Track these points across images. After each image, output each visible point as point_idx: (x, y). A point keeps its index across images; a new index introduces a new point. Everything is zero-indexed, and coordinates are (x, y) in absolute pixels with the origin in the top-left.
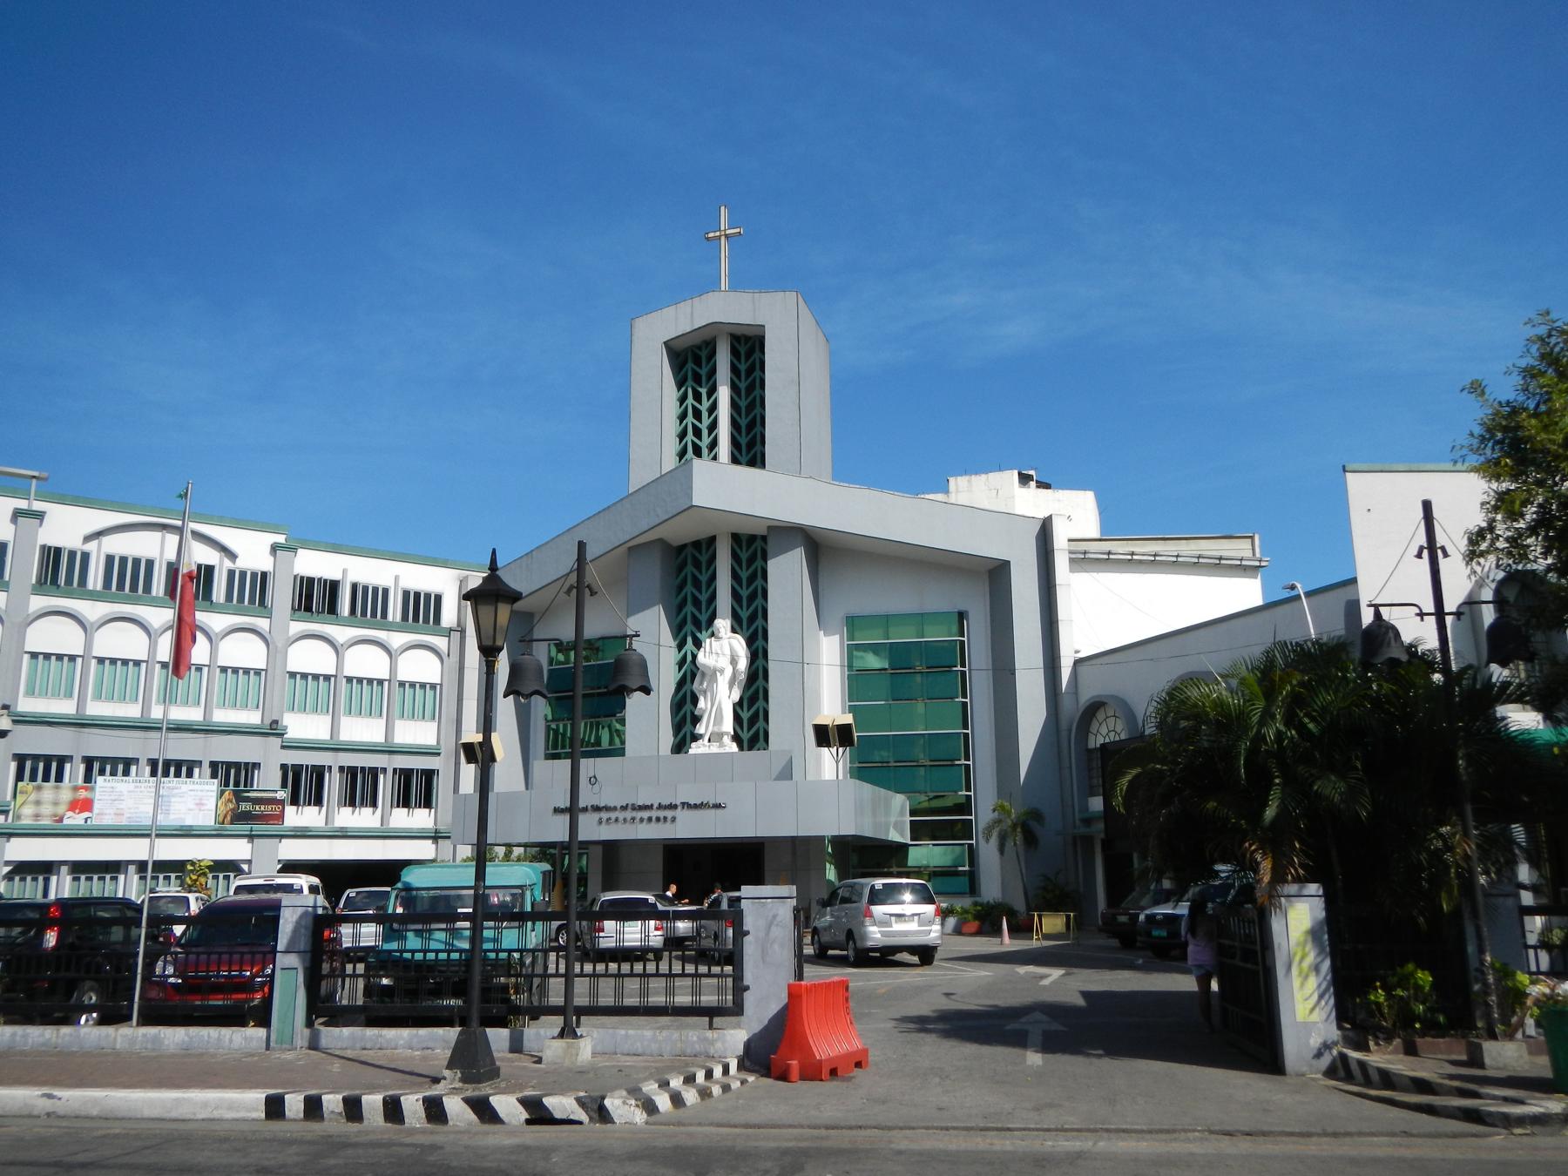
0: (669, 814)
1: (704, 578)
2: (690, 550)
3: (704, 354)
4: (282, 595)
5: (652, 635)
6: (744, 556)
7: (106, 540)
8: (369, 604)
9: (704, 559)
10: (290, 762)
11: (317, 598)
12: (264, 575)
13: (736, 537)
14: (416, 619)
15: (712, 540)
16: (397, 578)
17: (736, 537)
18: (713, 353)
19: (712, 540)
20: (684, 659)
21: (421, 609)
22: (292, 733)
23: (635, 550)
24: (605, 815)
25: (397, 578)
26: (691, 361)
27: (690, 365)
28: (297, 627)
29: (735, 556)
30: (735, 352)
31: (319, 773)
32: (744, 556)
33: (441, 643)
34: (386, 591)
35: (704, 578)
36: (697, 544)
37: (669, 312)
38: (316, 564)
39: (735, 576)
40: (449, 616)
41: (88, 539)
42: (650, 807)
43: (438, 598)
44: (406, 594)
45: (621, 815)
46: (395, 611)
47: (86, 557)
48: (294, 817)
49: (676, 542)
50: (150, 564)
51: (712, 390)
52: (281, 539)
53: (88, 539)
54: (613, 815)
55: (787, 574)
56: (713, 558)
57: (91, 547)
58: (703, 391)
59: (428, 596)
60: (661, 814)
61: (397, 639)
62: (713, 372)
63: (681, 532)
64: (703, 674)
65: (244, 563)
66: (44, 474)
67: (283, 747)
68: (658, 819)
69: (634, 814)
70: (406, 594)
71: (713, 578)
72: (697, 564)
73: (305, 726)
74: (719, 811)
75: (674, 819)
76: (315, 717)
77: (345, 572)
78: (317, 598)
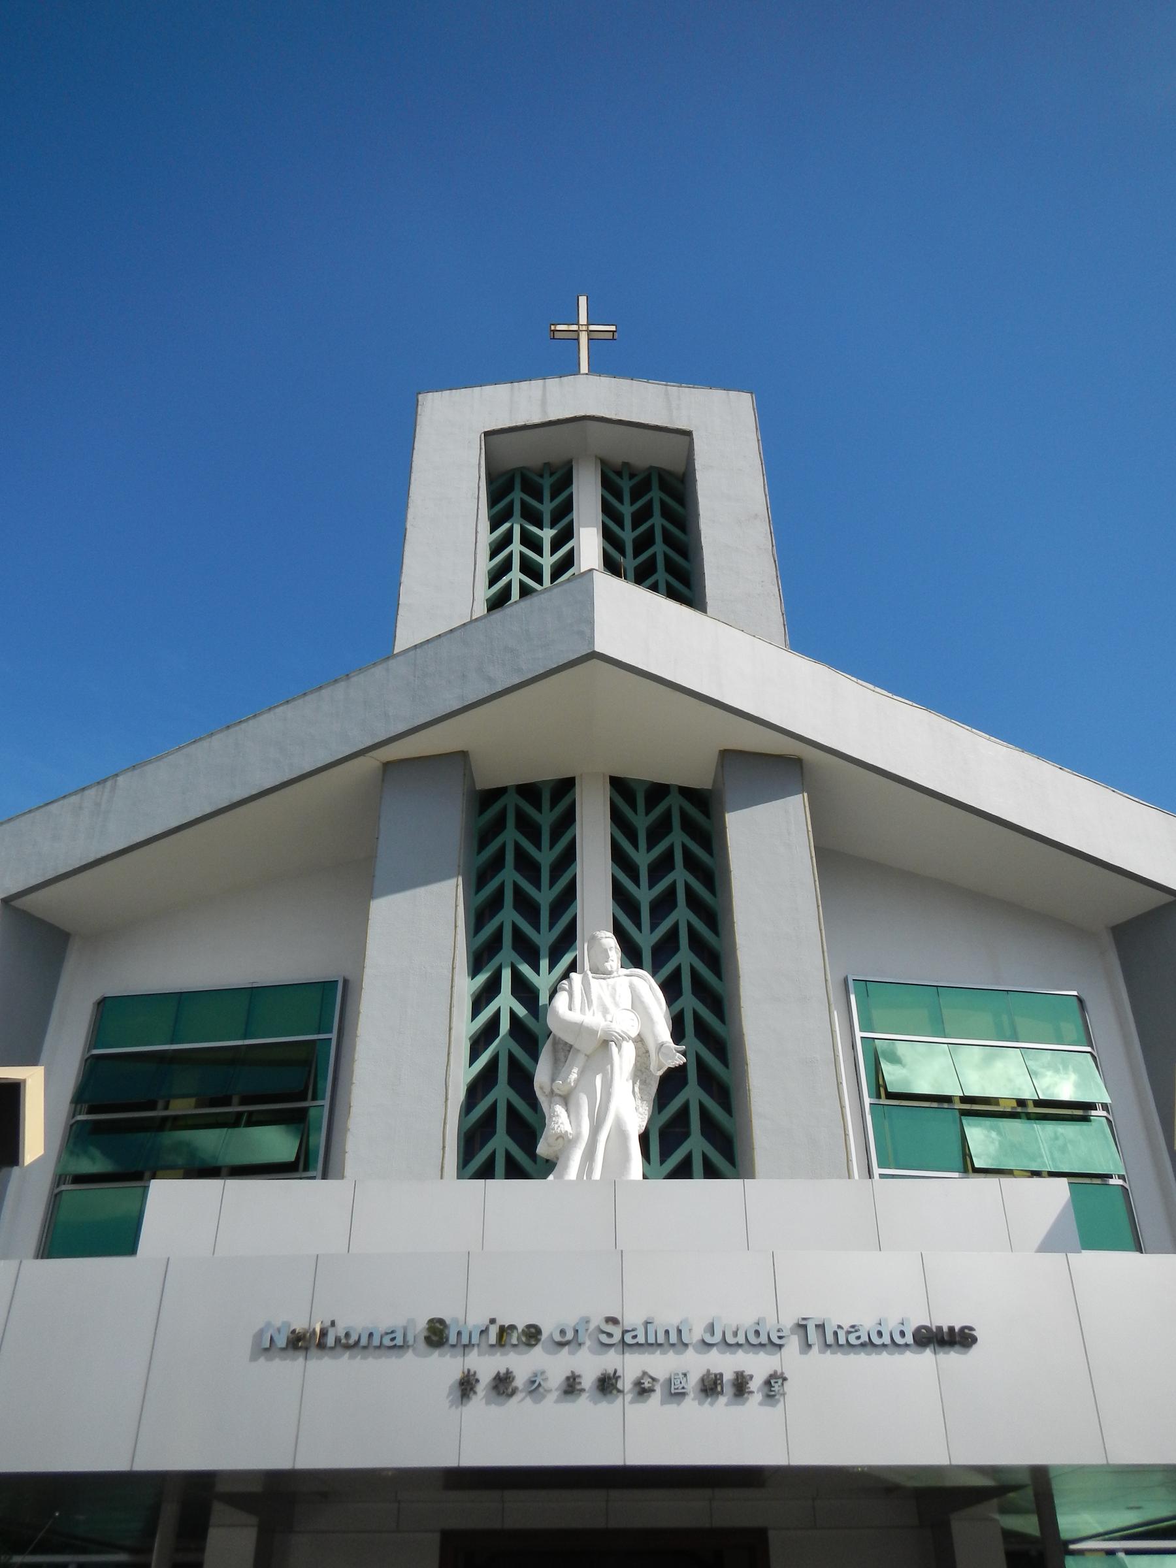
0: (758, 1366)
1: (546, 857)
2: (511, 801)
3: (547, 484)
5: (412, 969)
6: (642, 822)
9: (546, 819)
13: (618, 784)
15: (566, 785)
17: (618, 784)
18: (565, 480)
19: (566, 785)
20: (491, 1029)
23: (404, 771)
24: (486, 1366)
26: (525, 487)
27: (517, 496)
29: (617, 817)
30: (607, 483)
32: (642, 822)
35: (546, 857)
36: (529, 792)
37: (498, 393)
39: (619, 857)
42: (675, 1341)
45: (554, 1366)
49: (488, 780)
51: (566, 535)
54: (522, 1364)
55: (767, 851)
56: (568, 819)
58: (547, 535)
60: (726, 1364)
62: (567, 507)
63: (513, 748)
64: (563, 1051)
68: (711, 1387)
69: (610, 1361)
71: (569, 856)
72: (530, 829)
74: (952, 1358)
75: (773, 1385)
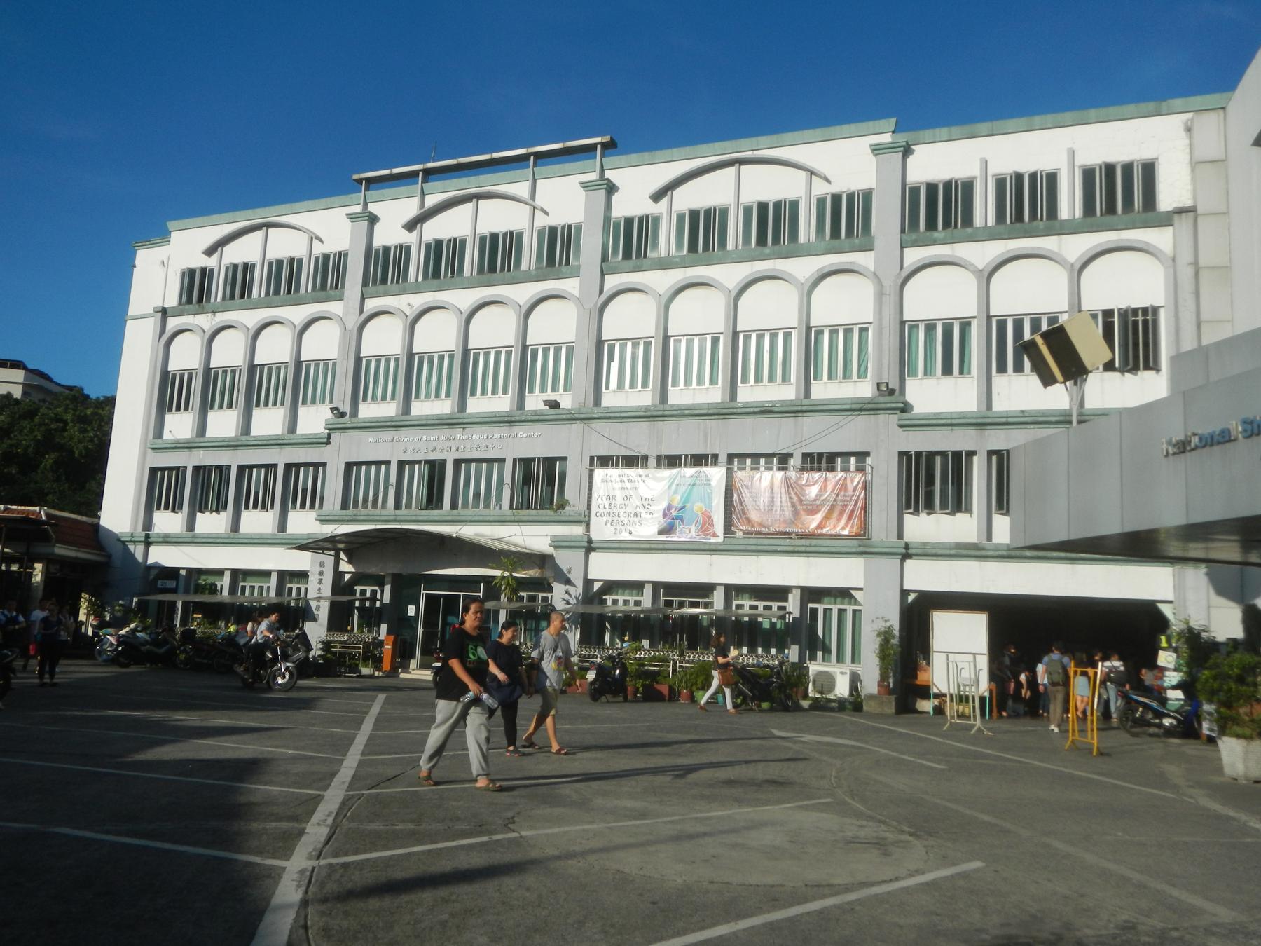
4: (886, 217)
7: (677, 193)
8: (1027, 203)
10: (912, 448)
11: (939, 211)
12: (867, 195)
14: (1111, 209)
16: (1072, 154)
21: (1121, 195)
22: (918, 409)
25: (1072, 154)
28: (914, 256)
31: (958, 462)
33: (1160, 238)
34: (1052, 178)
38: (940, 159)
40: (1173, 190)
41: (657, 197)
43: (1149, 169)
44: (1088, 174)
46: (1069, 204)
47: (657, 220)
48: (925, 527)
50: (724, 212)
52: (887, 138)
53: (657, 197)
57: (661, 208)
59: (1128, 168)
61: (1076, 246)
65: (835, 188)
66: (607, 138)
67: (901, 426)
70: (1088, 174)
73: (932, 394)
76: (948, 382)
77: (985, 163)
78: (939, 211)
